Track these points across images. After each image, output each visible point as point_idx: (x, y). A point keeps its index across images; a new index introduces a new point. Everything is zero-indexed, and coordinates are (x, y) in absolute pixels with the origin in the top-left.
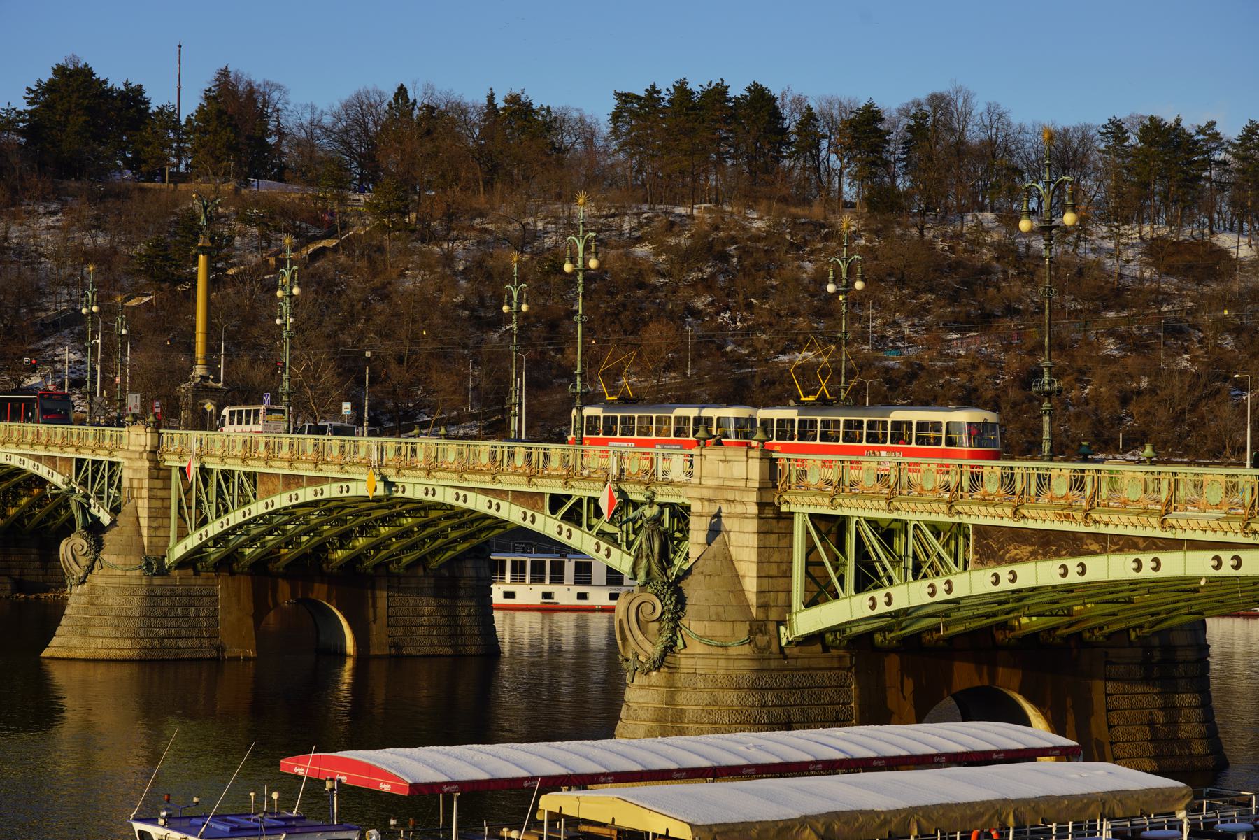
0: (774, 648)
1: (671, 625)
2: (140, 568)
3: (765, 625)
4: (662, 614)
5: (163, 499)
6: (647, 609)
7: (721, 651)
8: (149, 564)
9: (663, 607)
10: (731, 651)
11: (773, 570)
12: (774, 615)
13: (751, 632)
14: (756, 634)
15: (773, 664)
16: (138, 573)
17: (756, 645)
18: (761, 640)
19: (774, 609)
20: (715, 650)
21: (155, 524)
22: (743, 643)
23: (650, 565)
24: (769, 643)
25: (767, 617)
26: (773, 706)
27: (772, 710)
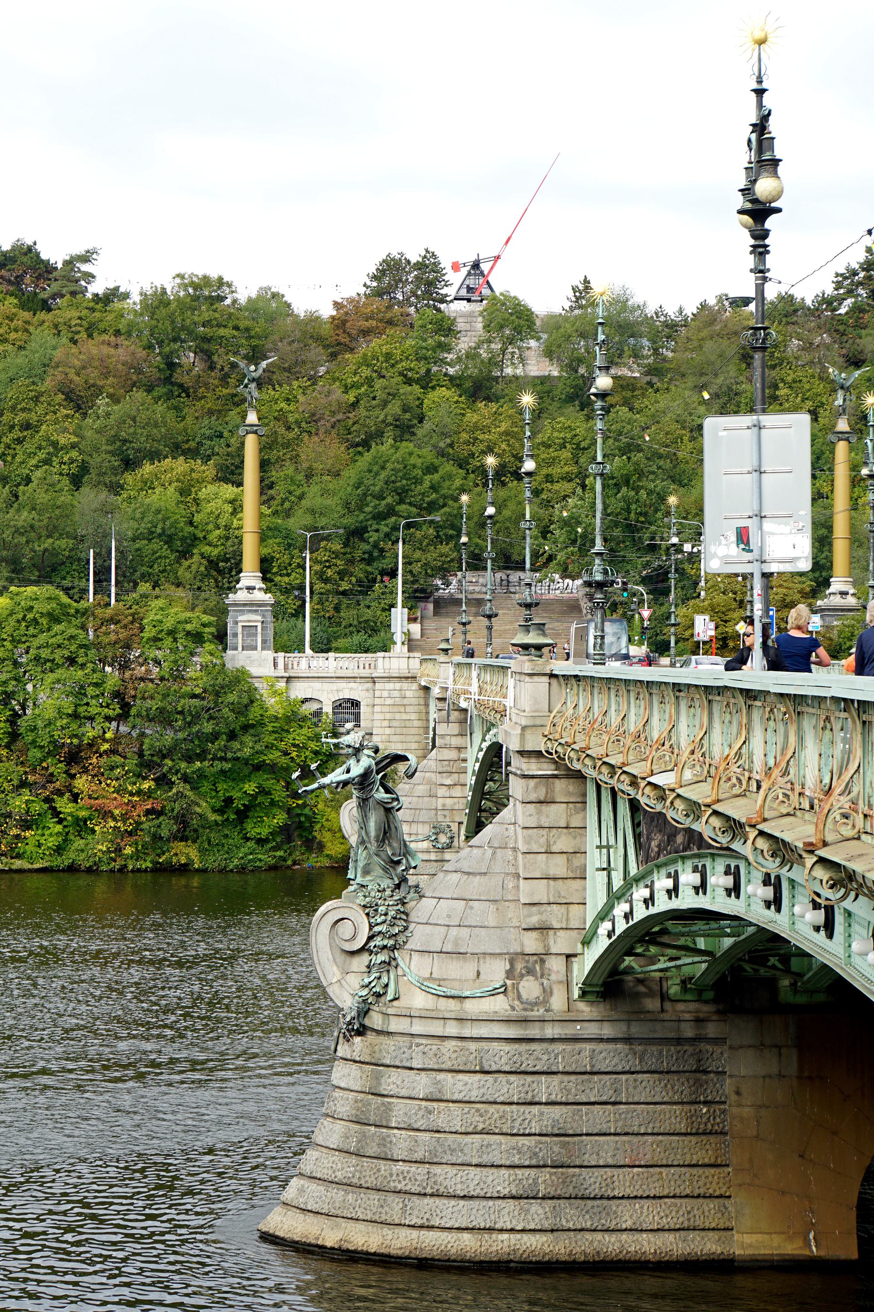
0: (558, 1002)
1: (381, 957)
2: (428, 838)
3: (543, 961)
4: (370, 938)
5: (459, 749)
6: (346, 929)
7: (452, 1004)
8: (438, 830)
9: (371, 927)
10: (472, 1008)
11: (558, 866)
12: (561, 943)
13: (510, 974)
14: (522, 976)
15: (550, 1031)
16: (425, 845)
17: (519, 997)
18: (530, 988)
19: (561, 933)
20: (443, 1003)
21: (448, 782)
22: (493, 993)
23: (369, 856)
24: (547, 992)
25: (547, 946)
26: (546, 1104)
27: (545, 1109)
